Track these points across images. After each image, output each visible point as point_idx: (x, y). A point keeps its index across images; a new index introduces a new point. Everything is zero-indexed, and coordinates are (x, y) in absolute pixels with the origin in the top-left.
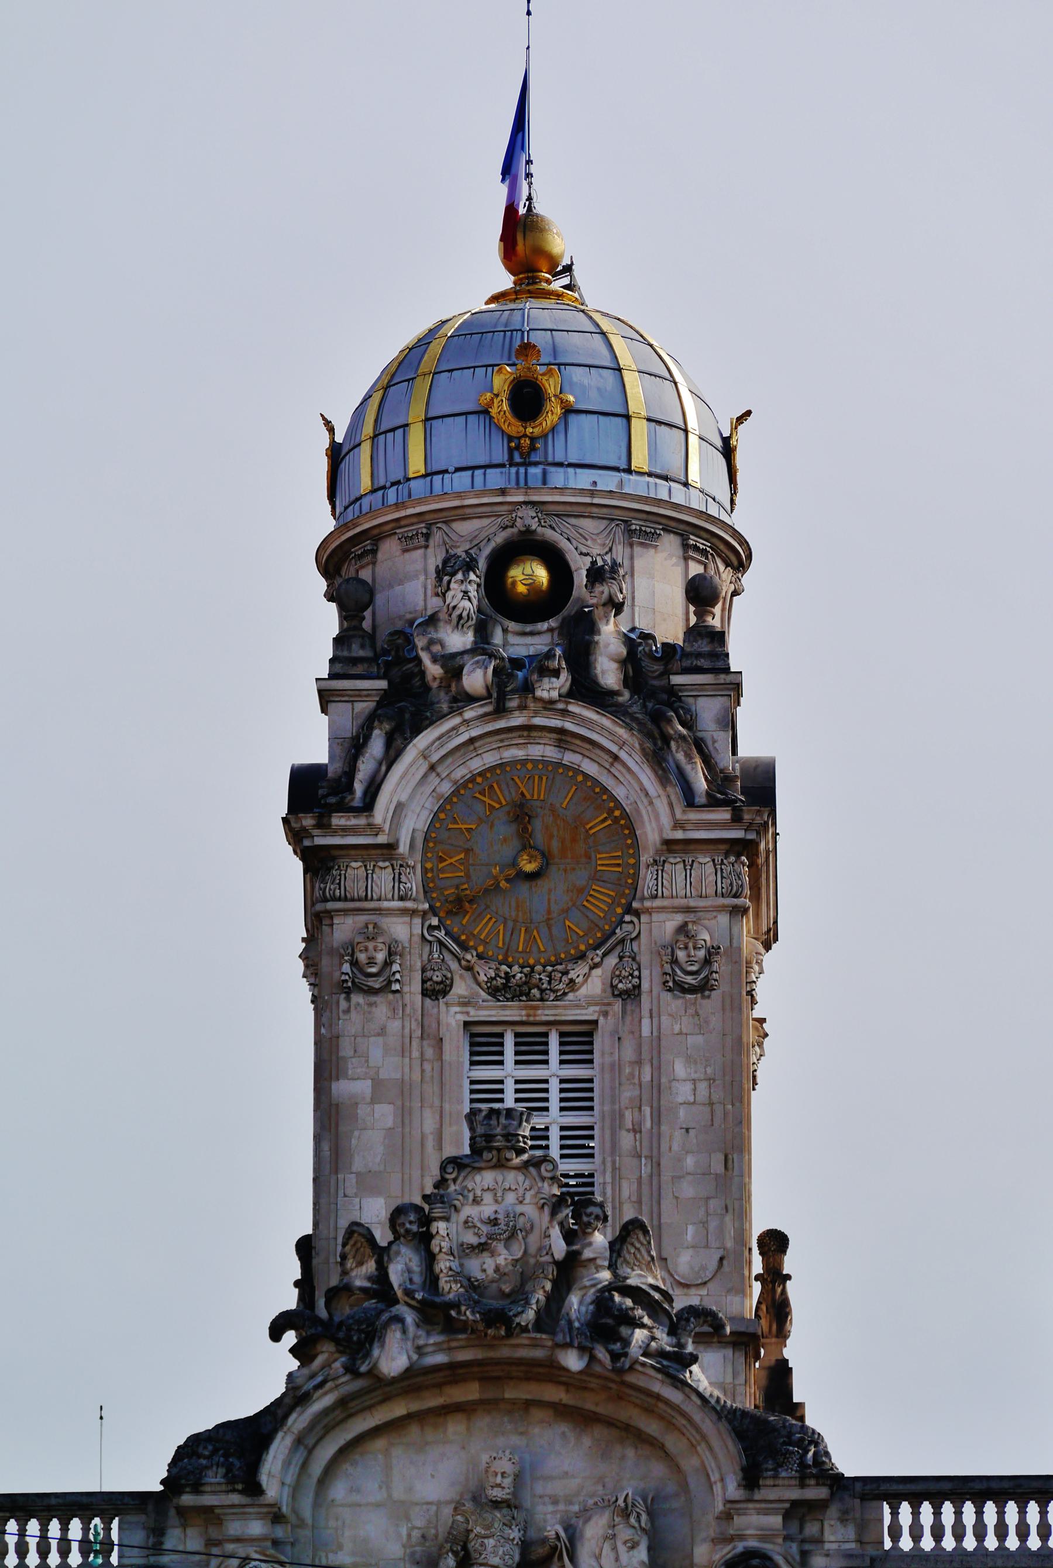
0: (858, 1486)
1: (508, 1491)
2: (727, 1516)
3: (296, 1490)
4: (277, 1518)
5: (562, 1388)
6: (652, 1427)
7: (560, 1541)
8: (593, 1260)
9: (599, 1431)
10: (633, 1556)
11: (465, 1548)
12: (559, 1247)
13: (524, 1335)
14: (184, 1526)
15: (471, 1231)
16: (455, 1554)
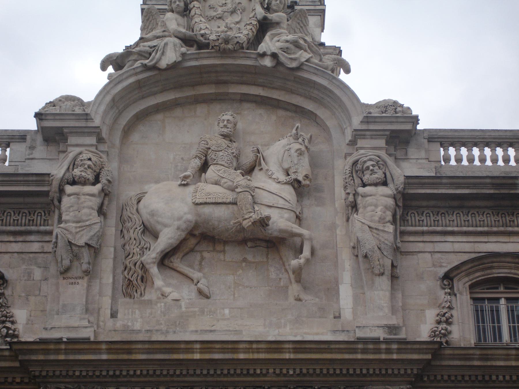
0: (426, 135)
1: (229, 130)
2: (353, 143)
3: (111, 129)
4: (100, 140)
5: (261, 88)
6: (310, 106)
7: (259, 153)
8: (278, 24)
9: (281, 113)
10: (301, 159)
11: (206, 156)
12: (260, 12)
13: (241, 51)
14: (48, 145)
15: (212, 10)
16: (200, 159)
